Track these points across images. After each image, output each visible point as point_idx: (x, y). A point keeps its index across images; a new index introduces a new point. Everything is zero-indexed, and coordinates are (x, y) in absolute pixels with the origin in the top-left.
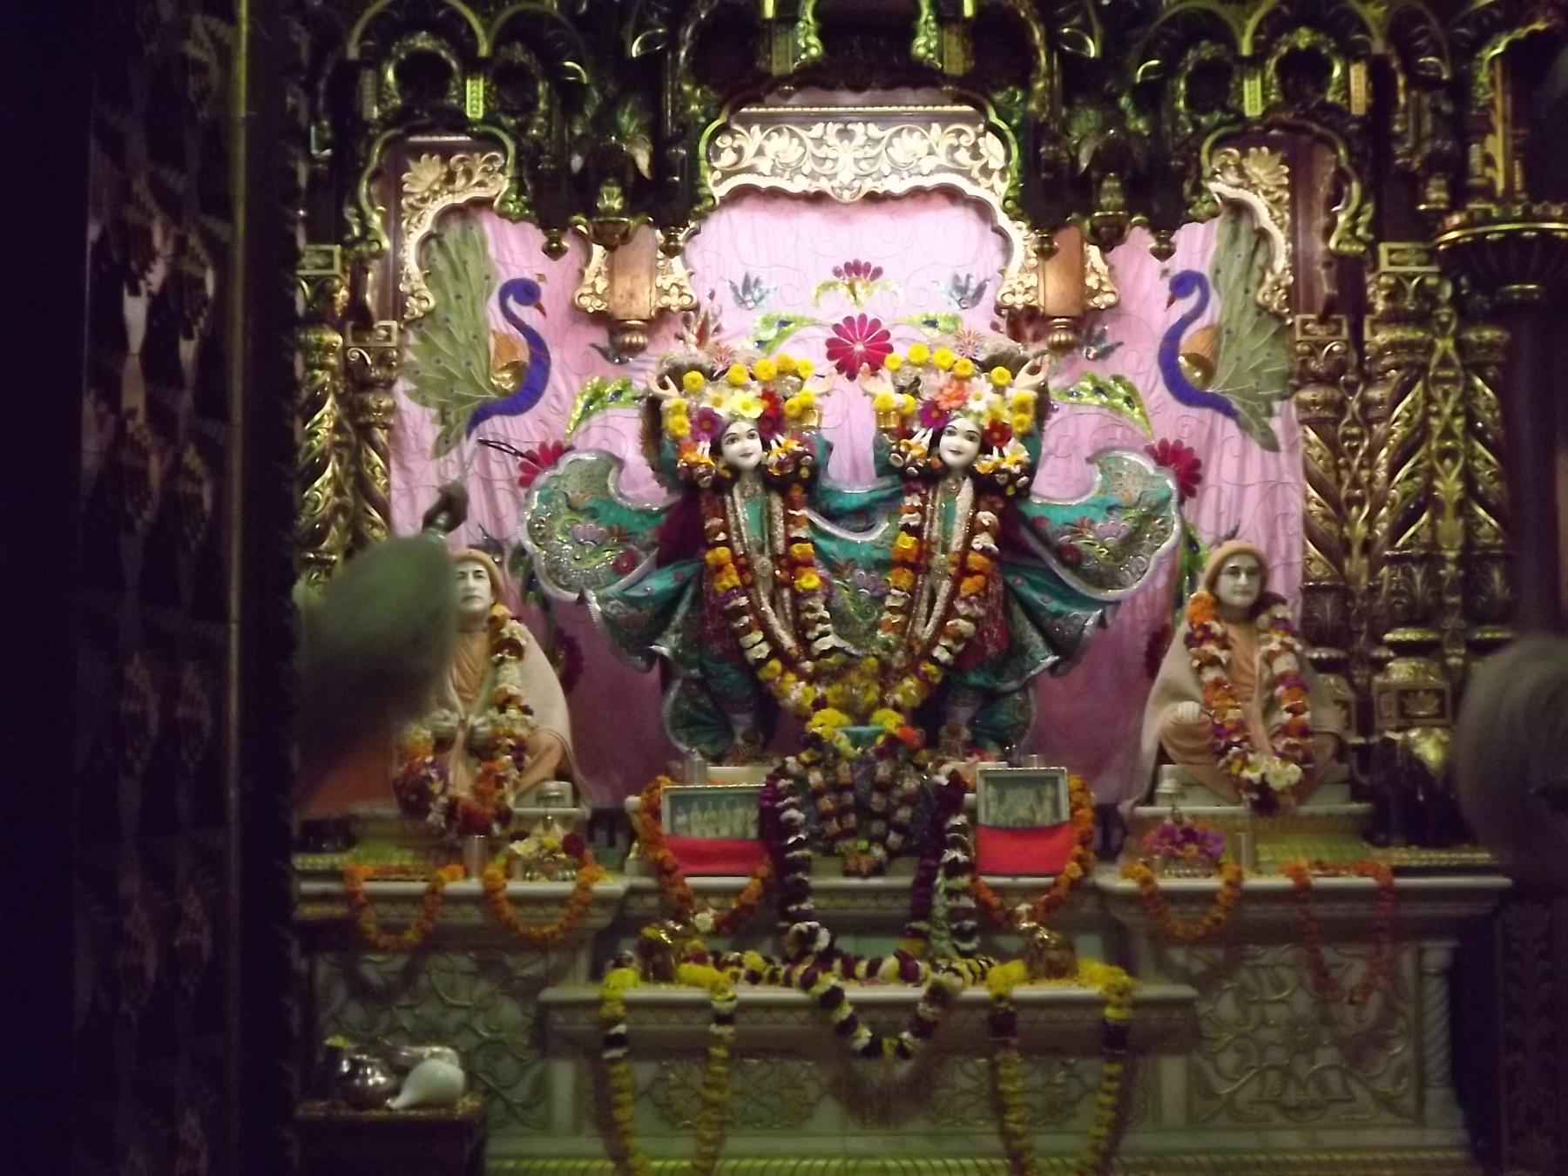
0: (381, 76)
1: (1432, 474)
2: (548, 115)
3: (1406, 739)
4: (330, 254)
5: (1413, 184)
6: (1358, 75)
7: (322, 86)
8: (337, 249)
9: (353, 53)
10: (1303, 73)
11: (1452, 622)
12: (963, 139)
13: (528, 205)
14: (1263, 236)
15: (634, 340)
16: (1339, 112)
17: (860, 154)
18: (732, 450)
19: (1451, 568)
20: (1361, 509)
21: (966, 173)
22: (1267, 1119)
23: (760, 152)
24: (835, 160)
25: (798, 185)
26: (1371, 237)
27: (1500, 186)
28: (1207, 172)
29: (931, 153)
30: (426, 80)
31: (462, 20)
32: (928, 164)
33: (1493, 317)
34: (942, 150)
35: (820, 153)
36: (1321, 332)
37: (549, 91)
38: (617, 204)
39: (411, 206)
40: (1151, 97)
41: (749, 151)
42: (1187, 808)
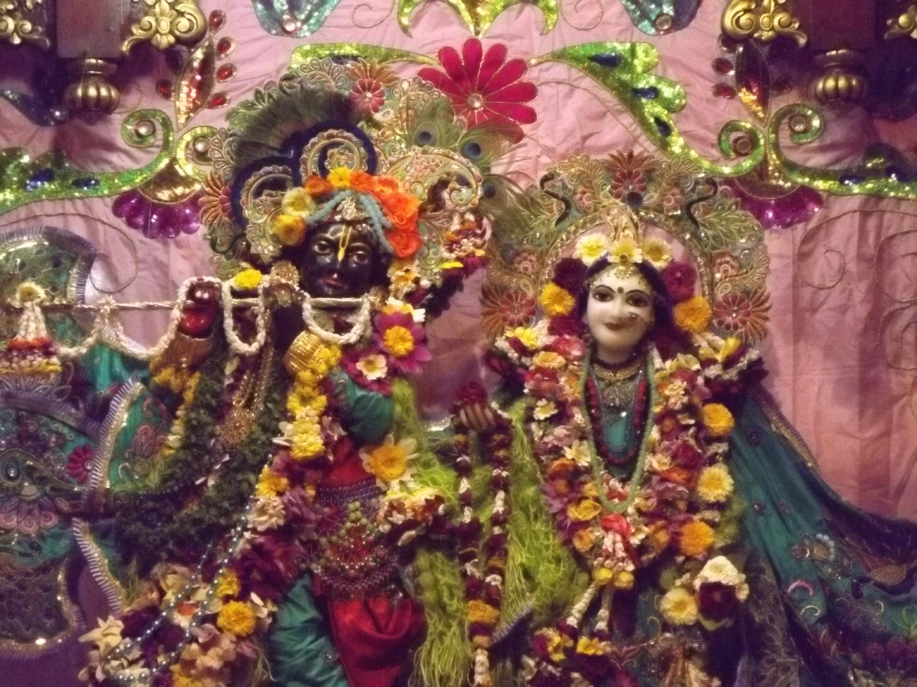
15: (92, 92)
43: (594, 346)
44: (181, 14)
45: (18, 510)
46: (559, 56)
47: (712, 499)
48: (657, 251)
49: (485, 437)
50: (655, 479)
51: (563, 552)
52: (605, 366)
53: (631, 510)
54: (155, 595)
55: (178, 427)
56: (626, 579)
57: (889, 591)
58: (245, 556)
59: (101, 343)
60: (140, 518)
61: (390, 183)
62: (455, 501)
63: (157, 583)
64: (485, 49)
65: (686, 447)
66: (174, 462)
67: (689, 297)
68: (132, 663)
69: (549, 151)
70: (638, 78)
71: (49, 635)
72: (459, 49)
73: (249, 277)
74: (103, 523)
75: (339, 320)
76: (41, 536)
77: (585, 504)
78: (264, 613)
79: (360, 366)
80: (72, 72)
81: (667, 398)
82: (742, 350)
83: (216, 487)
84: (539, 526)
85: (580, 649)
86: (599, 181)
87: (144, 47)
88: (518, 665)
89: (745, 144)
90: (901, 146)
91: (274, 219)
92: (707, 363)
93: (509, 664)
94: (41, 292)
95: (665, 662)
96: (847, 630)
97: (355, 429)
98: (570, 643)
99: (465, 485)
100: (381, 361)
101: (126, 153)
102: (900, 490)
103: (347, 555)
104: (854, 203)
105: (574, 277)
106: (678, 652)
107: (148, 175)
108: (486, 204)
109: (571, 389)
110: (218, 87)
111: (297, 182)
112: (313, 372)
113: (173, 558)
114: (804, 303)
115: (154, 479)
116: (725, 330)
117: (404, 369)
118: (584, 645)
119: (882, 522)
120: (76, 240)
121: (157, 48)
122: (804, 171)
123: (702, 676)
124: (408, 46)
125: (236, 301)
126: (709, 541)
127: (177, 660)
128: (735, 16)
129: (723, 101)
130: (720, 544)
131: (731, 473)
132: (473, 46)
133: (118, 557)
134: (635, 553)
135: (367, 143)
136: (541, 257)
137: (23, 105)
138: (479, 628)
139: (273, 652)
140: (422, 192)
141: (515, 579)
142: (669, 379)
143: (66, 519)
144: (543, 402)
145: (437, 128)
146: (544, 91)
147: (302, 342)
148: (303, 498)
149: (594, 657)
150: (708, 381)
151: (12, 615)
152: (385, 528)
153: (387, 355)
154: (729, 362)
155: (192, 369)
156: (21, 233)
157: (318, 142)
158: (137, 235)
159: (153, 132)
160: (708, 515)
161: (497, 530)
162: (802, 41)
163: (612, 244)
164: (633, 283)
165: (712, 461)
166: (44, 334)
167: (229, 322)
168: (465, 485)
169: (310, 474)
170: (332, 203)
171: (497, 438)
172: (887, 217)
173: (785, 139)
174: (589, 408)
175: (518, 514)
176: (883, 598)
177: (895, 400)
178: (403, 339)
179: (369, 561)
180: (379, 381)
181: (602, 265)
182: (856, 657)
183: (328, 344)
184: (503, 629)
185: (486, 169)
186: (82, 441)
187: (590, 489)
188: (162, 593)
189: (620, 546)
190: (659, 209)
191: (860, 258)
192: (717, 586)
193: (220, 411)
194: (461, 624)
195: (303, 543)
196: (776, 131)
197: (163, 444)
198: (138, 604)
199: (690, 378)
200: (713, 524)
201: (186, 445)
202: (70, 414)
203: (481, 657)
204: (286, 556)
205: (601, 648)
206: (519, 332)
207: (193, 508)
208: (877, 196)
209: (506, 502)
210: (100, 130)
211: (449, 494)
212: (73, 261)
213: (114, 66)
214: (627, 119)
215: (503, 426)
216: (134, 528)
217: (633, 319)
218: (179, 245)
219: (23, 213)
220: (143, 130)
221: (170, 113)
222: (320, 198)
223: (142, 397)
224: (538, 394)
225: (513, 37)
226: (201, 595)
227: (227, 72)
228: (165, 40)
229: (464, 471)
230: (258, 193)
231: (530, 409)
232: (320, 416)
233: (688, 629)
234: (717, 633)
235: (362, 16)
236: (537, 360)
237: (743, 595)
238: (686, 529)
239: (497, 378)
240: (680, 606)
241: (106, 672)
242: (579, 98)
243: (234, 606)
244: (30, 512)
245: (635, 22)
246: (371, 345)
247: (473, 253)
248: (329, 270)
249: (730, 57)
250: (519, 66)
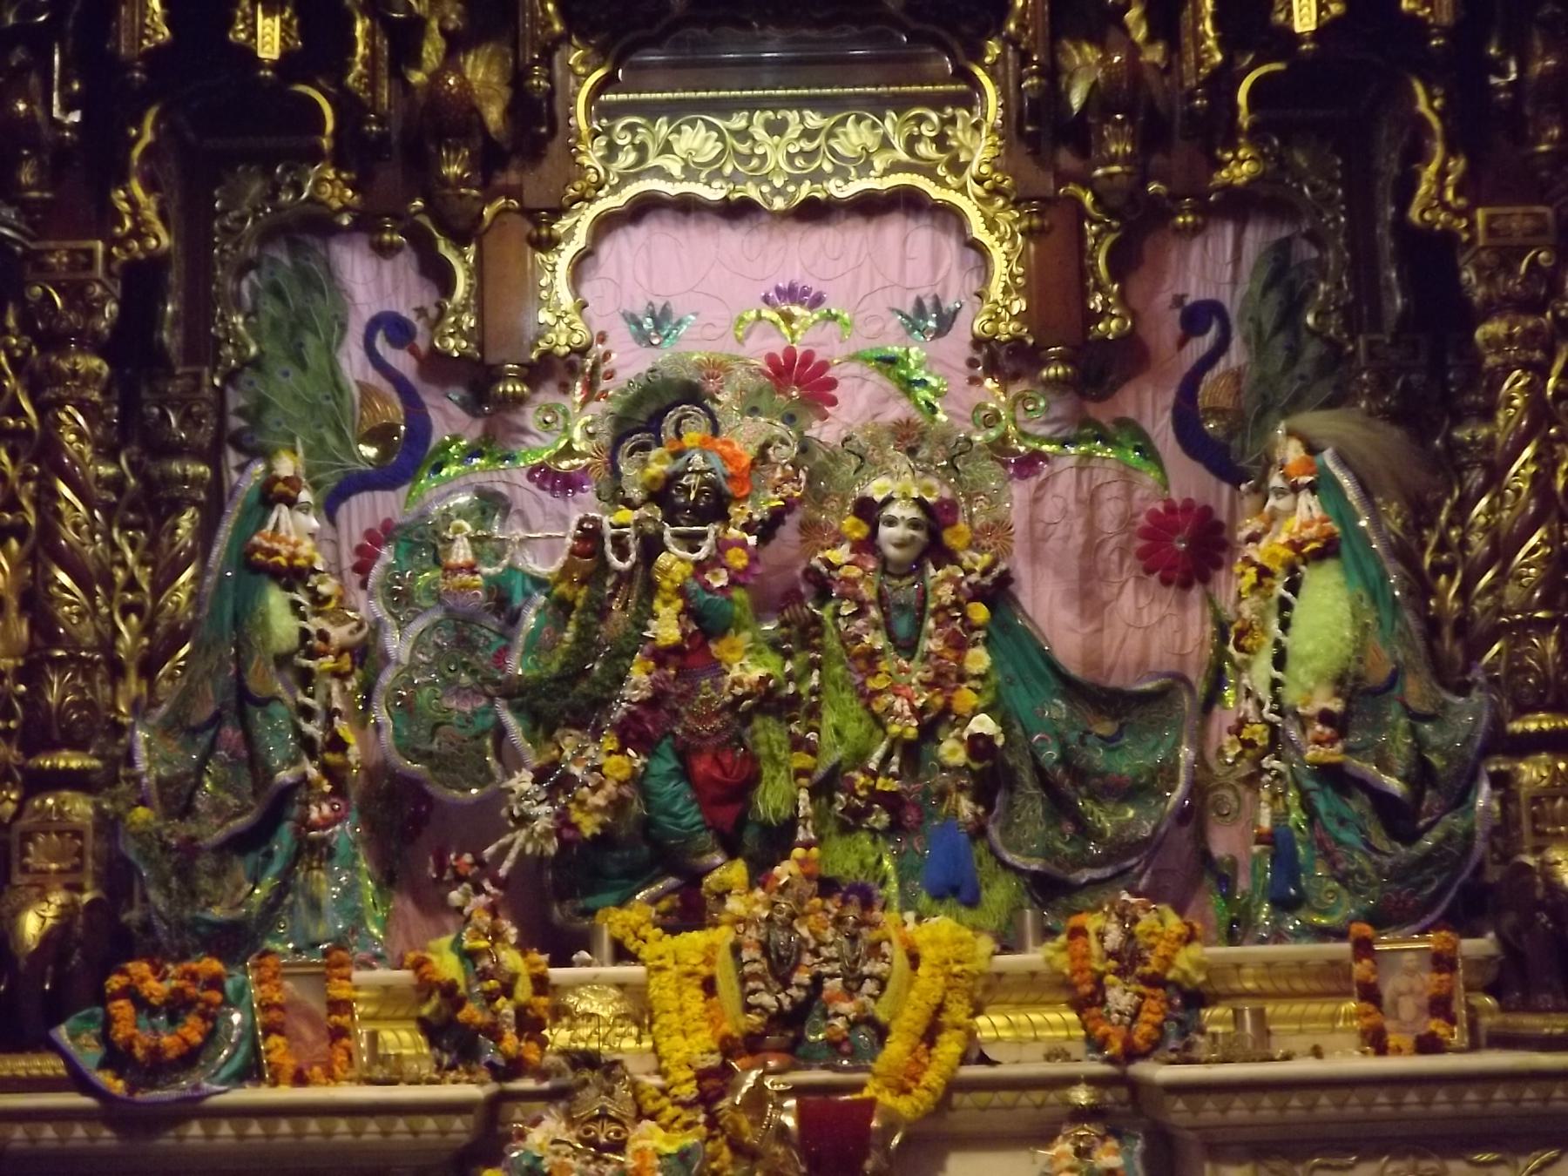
3: (1543, 863)
4: (90, 253)
7: (70, 24)
12: (926, 130)
15: (510, 388)
17: (792, 149)
20: (1451, 579)
21: (929, 171)
24: (764, 157)
25: (714, 193)
26: (1461, 202)
29: (886, 144)
34: (898, 142)
35: (744, 148)
37: (370, 34)
39: (225, 229)
43: (884, 561)
44: (574, 331)
45: (456, 693)
46: (853, 358)
47: (975, 672)
48: (929, 490)
49: (803, 630)
50: (932, 657)
51: (863, 714)
52: (893, 575)
53: (914, 680)
54: (556, 752)
55: (572, 627)
56: (911, 733)
57: (1107, 741)
58: (623, 721)
59: (511, 568)
60: (546, 696)
61: (729, 443)
62: (782, 678)
63: (557, 743)
64: (799, 354)
65: (954, 631)
66: (568, 653)
67: (954, 523)
68: (540, 803)
69: (849, 425)
70: (912, 372)
71: (480, 785)
72: (780, 354)
73: (626, 515)
74: (519, 700)
75: (692, 541)
76: (474, 713)
77: (880, 676)
78: (638, 763)
79: (708, 577)
80: (494, 374)
81: (940, 598)
82: (995, 563)
83: (602, 671)
84: (846, 695)
85: (879, 787)
86: (884, 441)
87: (547, 356)
88: (832, 801)
89: (991, 420)
90: (1104, 421)
91: (643, 472)
92: (968, 572)
93: (824, 800)
94: (468, 527)
95: (943, 794)
96: (1076, 769)
97: (706, 624)
98: (872, 782)
99: (789, 666)
100: (724, 573)
101: (536, 435)
102: (1111, 669)
103: (700, 719)
104: (1071, 461)
105: (868, 510)
106: (952, 787)
107: (553, 451)
108: (802, 459)
109: (867, 592)
110: (604, 384)
111: (659, 444)
112: (673, 581)
113: (569, 725)
114: (1038, 533)
115: (555, 667)
116: (981, 550)
117: (741, 579)
118: (882, 784)
119: (1103, 689)
120: (498, 495)
121: (557, 356)
122: (1035, 438)
123: (971, 805)
124: (742, 353)
125: (614, 531)
126: (974, 702)
127: (573, 799)
128: (981, 325)
129: (974, 389)
130: (982, 704)
131: (989, 652)
132: (790, 352)
133: (529, 725)
134: (919, 713)
135: (711, 415)
136: (844, 501)
137: (464, 405)
138: (801, 773)
139: (646, 793)
140: (751, 452)
141: (828, 736)
142: (941, 584)
143: (491, 698)
144: (846, 602)
145: (763, 403)
146: (843, 383)
147: (663, 560)
148: (667, 677)
149: (891, 792)
150: (969, 585)
151: (454, 771)
152: (729, 698)
153: (728, 568)
154: (986, 572)
155: (582, 582)
156: (458, 491)
157: (673, 415)
158: (545, 496)
159: (556, 419)
160: (973, 684)
161: (814, 699)
162: (1030, 341)
163: (897, 487)
164: (912, 513)
165: (975, 644)
166: (470, 558)
167: (608, 546)
168: (789, 666)
169: (673, 659)
170: (685, 458)
171: (813, 629)
172: (1096, 472)
173: (1020, 416)
174: (881, 607)
175: (830, 688)
176: (1102, 746)
177: (1105, 604)
178: (740, 557)
179: (717, 723)
180: (722, 587)
181: (889, 500)
182: (1083, 790)
183: (682, 560)
184: (821, 772)
185: (801, 433)
186: (503, 642)
187: (883, 666)
188: (561, 751)
189: (907, 707)
190: (930, 461)
191: (1078, 501)
192: (981, 735)
193: (603, 613)
194: (788, 770)
195: (668, 711)
196: (1013, 410)
197: (561, 640)
198: (544, 759)
199: (957, 582)
200: (977, 691)
201: (578, 639)
202: (493, 622)
203: (804, 795)
204: (654, 722)
205: (892, 786)
206: (828, 553)
207: (584, 686)
208: (1088, 456)
209: (820, 677)
210: (516, 419)
211: (778, 673)
212: (496, 509)
213: (526, 371)
214: (905, 402)
215: (817, 621)
216: (541, 702)
217: (913, 538)
218: (575, 501)
219: (462, 482)
220: (548, 419)
221: (568, 405)
222: (677, 455)
223: (545, 606)
224: (842, 597)
225: (820, 344)
226: (590, 752)
227: (610, 375)
228: (564, 350)
229: (788, 655)
230: (631, 453)
231: (838, 607)
232: (679, 614)
233: (957, 770)
234: (983, 770)
235: (709, 332)
236: (841, 572)
237: (1000, 742)
238: (956, 695)
239: (813, 588)
240: (953, 752)
241: (521, 810)
242: (869, 388)
243: (615, 758)
244: (466, 696)
245: (909, 332)
246: (715, 561)
247: (791, 496)
248: (684, 508)
249: (978, 357)
250: (824, 366)
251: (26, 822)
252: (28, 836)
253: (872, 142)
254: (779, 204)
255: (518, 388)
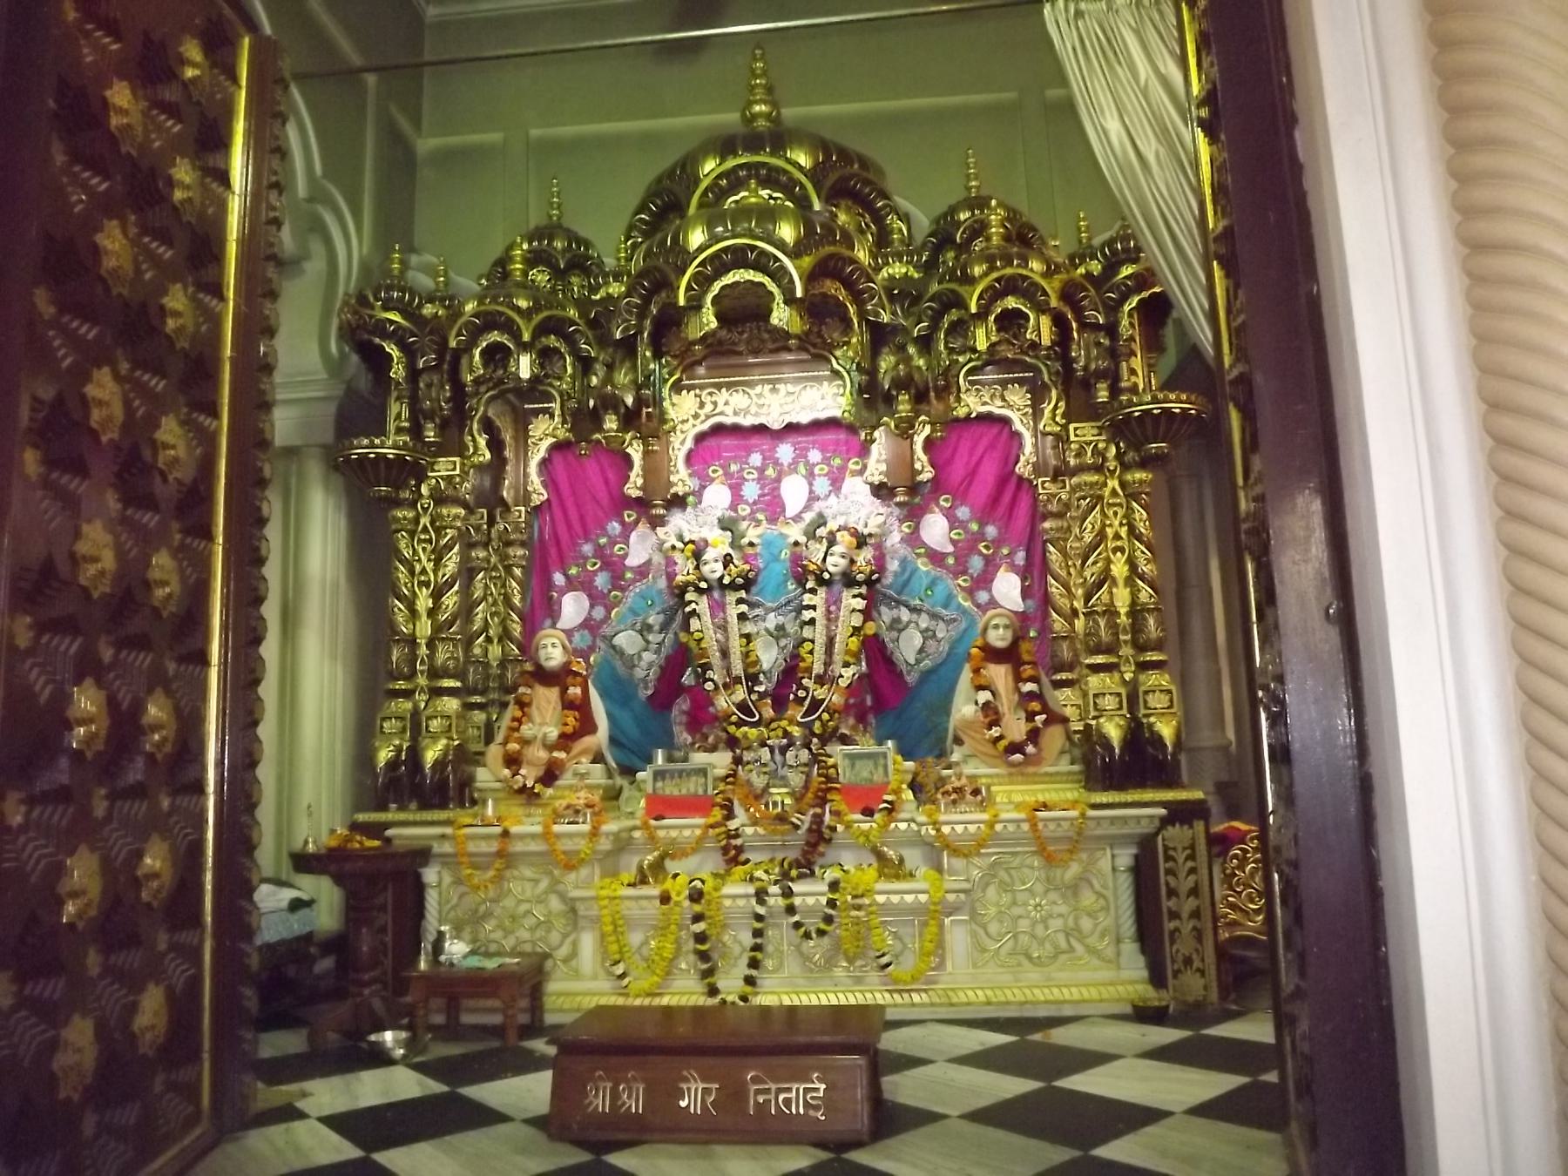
0: (472, 357)
1: (1109, 561)
2: (573, 377)
5: (1087, 385)
6: (1045, 322)
8: (457, 459)
9: (453, 344)
10: (1011, 322)
11: (1126, 651)
13: (568, 430)
14: (1018, 435)
16: (1035, 346)
18: (705, 569)
19: (1124, 618)
22: (1019, 965)
23: (726, 403)
25: (747, 421)
27: (1141, 387)
28: (963, 389)
30: (496, 355)
31: (513, 321)
32: (822, 404)
33: (1143, 464)
36: (1052, 488)
38: (614, 426)
40: (925, 343)
41: (721, 403)
42: (968, 770)
251: (429, 712)
252: (429, 718)
253: (819, 395)
254: (776, 426)
255: (662, 511)
